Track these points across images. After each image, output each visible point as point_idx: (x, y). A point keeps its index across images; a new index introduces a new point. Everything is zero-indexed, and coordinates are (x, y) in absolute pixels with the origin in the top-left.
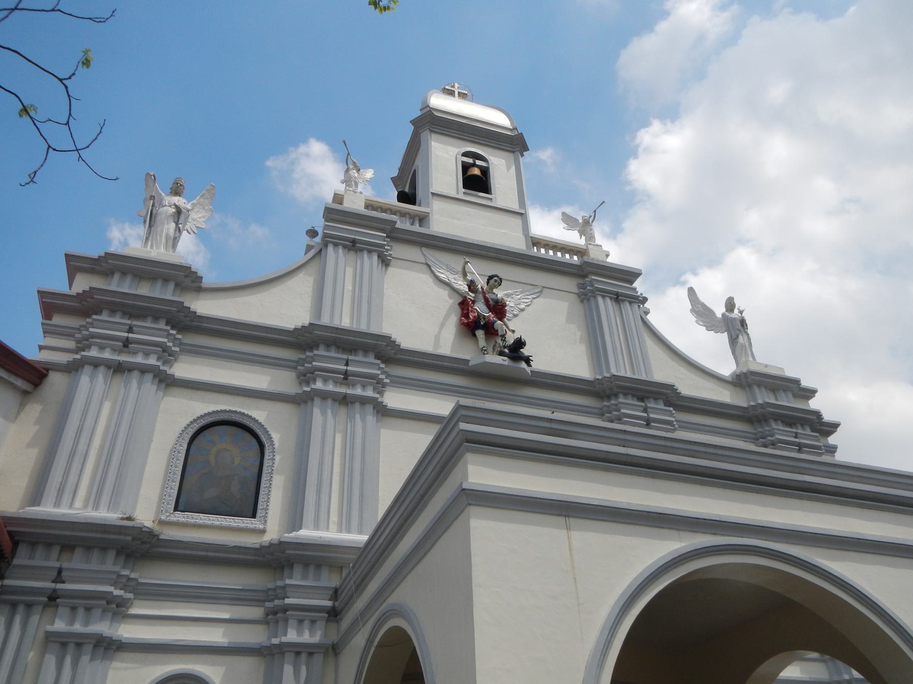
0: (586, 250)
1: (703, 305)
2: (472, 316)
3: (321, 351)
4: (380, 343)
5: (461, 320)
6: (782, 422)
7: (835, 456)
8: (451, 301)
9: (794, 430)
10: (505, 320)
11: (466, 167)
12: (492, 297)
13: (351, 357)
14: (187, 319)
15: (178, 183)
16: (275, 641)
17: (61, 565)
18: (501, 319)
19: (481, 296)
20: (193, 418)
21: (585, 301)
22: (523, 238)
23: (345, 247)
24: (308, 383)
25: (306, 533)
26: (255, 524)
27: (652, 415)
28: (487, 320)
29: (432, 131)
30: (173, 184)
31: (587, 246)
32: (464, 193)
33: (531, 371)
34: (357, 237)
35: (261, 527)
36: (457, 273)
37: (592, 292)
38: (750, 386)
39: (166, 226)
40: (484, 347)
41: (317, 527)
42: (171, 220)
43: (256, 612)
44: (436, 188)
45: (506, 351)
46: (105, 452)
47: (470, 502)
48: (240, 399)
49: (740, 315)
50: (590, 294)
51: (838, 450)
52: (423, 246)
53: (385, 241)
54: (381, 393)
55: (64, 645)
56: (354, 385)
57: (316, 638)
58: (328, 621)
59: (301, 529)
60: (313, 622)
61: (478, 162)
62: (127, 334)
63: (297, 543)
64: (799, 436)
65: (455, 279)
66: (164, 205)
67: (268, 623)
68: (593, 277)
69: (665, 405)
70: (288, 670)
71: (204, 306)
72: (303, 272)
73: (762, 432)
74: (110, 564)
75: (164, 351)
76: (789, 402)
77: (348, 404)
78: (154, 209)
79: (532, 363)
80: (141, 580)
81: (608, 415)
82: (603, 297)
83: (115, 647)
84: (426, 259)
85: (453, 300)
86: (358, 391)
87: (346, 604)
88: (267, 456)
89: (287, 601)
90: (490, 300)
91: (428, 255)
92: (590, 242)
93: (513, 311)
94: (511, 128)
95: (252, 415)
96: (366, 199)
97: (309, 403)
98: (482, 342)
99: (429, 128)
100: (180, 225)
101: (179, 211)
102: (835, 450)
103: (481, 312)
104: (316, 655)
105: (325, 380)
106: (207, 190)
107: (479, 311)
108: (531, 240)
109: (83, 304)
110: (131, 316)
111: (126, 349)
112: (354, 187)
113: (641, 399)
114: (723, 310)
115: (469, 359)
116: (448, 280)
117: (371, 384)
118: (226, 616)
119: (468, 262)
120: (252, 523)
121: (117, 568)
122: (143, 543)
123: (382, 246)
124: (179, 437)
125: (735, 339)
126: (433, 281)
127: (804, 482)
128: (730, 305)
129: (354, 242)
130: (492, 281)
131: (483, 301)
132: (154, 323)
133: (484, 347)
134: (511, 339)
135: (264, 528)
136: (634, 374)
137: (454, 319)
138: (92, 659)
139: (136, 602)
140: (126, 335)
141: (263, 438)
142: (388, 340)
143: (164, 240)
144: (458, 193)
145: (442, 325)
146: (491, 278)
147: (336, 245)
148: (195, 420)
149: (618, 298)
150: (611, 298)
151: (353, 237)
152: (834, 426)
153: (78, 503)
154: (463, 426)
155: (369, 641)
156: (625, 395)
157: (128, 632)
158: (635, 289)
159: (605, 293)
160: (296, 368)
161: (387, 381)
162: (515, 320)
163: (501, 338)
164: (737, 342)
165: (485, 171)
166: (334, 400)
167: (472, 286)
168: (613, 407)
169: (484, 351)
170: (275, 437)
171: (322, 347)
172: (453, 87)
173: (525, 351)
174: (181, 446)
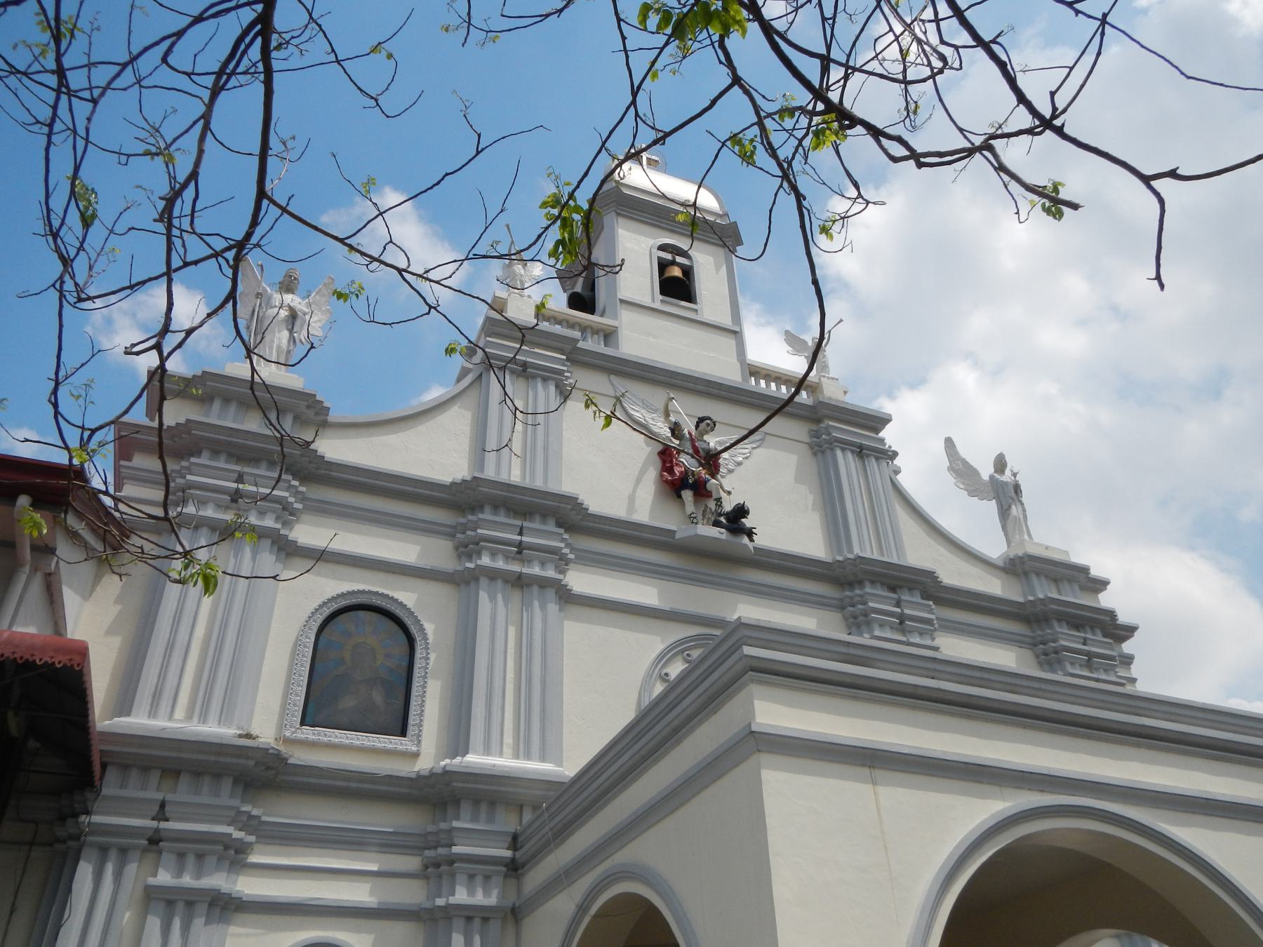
0: (818, 383)
1: (965, 462)
3: (487, 515)
4: (562, 505)
5: (662, 476)
6: (1068, 623)
7: (1130, 668)
8: (649, 449)
9: (1083, 635)
10: (719, 476)
11: (663, 266)
13: (526, 524)
14: (312, 465)
15: (291, 276)
16: (440, 902)
17: (164, 798)
18: (713, 476)
20: (322, 600)
21: (819, 454)
24: (470, 557)
25: (475, 759)
26: (406, 745)
27: (907, 611)
28: (696, 477)
29: (618, 214)
30: (285, 277)
31: (820, 379)
32: (661, 301)
33: (754, 548)
34: (528, 360)
35: (414, 749)
36: (655, 411)
38: (1026, 574)
39: (277, 334)
40: (693, 513)
41: (487, 751)
42: (284, 326)
43: (411, 863)
44: (624, 293)
45: (723, 519)
46: (213, 644)
47: (760, 748)
48: (381, 576)
49: (1013, 478)
50: (826, 445)
51: (1135, 661)
52: (613, 374)
53: (564, 365)
54: (563, 572)
55: (170, 903)
56: (529, 562)
57: (492, 900)
58: (506, 876)
59: (468, 753)
60: (487, 878)
61: (679, 259)
62: (236, 484)
63: (467, 773)
64: (1088, 642)
65: (653, 419)
66: (273, 305)
67: (427, 878)
68: (831, 423)
69: (923, 598)
70: (458, 941)
71: (333, 448)
73: (1042, 636)
74: (226, 797)
75: (284, 509)
76: (1075, 597)
77: (523, 587)
78: (260, 311)
80: (264, 818)
81: (850, 609)
82: (843, 450)
83: (233, 907)
86: (536, 570)
87: (534, 856)
88: (419, 653)
89: (455, 849)
91: (618, 385)
92: (823, 374)
94: (721, 213)
95: (398, 598)
97: (473, 585)
98: (690, 506)
100: (295, 334)
101: (293, 316)
102: (1130, 661)
104: (492, 921)
105: (493, 555)
106: (325, 284)
109: (174, 441)
110: (239, 459)
111: (234, 505)
113: (893, 589)
114: (992, 470)
115: (676, 529)
116: (645, 420)
117: (552, 561)
118: (374, 867)
119: (673, 398)
120: (402, 744)
121: (235, 802)
122: (269, 768)
123: (561, 372)
124: (305, 626)
125: (1007, 510)
127: (1143, 726)
128: (1000, 464)
130: (703, 425)
132: (269, 471)
133: (693, 513)
134: (728, 507)
135: (418, 750)
136: (883, 555)
137: (652, 474)
138: (207, 923)
139: (257, 847)
140: (235, 485)
141: (413, 630)
142: (572, 502)
144: (653, 300)
145: (638, 481)
146: (701, 420)
148: (324, 604)
149: (861, 452)
150: (853, 452)
151: (524, 359)
152: (1130, 631)
153: (180, 713)
154: (748, 650)
155: (582, 909)
156: (873, 582)
157: (249, 886)
158: (882, 441)
159: (845, 445)
160: (453, 536)
161: (572, 556)
162: (729, 476)
163: (716, 502)
164: (1009, 514)
165: (688, 272)
166: (506, 582)
167: (676, 430)
168: (859, 599)
169: (692, 519)
170: (429, 628)
171: (488, 509)
173: (748, 522)
174: (307, 637)
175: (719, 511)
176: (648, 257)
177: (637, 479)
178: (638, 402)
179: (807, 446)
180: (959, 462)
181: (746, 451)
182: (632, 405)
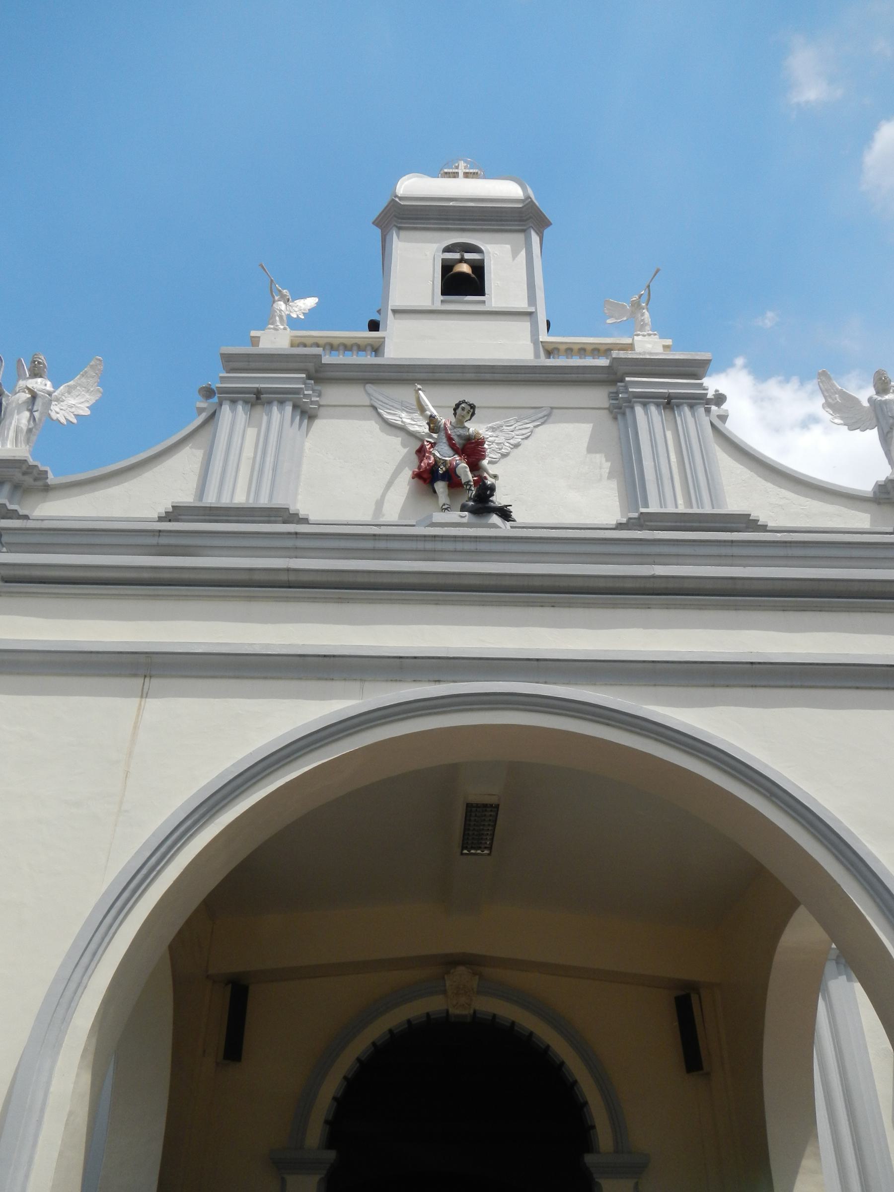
11: (447, 267)
12: (458, 433)
19: (442, 434)
21: (619, 417)
23: (246, 402)
29: (400, 228)
31: (633, 339)
37: (628, 401)
39: (16, 417)
40: (444, 505)
50: (624, 404)
52: (367, 383)
61: (468, 256)
65: (412, 419)
72: (190, 445)
79: (514, 515)
82: (645, 405)
84: (371, 399)
85: (408, 449)
90: (455, 438)
96: (292, 336)
99: (395, 225)
101: (34, 396)
103: (440, 457)
107: (438, 455)
108: (543, 347)
112: (278, 324)
114: (871, 392)
125: (888, 433)
129: (258, 393)
130: (459, 411)
131: (445, 440)
133: (444, 505)
143: (12, 434)
146: (458, 406)
147: (234, 401)
149: (669, 403)
150: (658, 405)
151: (257, 386)
159: (646, 399)
165: (479, 269)
172: (457, 168)
175: (470, 496)
176: (432, 261)
177: (388, 482)
178: (396, 405)
179: (606, 412)
180: (837, 396)
181: (528, 430)
182: (390, 409)
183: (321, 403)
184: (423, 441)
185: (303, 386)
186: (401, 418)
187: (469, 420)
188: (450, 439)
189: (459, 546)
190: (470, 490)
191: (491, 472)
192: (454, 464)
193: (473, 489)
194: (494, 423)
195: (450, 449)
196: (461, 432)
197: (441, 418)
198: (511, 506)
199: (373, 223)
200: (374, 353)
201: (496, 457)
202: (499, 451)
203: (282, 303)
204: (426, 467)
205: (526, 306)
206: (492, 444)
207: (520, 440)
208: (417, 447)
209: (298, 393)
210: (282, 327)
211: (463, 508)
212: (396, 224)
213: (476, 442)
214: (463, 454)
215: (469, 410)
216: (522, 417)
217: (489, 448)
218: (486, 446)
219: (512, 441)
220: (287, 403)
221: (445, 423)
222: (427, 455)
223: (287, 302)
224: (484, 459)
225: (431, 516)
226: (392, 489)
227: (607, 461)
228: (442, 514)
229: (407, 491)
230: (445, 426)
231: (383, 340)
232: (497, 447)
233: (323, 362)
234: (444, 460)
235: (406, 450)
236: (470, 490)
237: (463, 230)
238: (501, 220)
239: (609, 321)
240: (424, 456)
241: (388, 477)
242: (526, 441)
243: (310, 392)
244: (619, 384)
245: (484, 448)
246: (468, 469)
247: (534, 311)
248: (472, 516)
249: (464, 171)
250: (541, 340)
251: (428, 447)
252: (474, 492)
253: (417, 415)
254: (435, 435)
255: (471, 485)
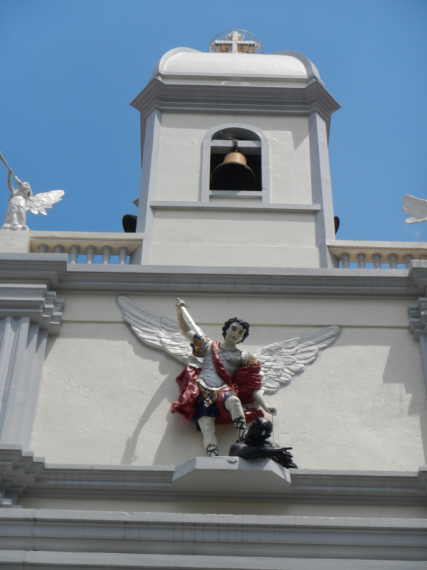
2: (187, 395)
12: (228, 358)
19: (209, 358)
22: (316, 251)
28: (214, 399)
29: (162, 111)
33: (293, 476)
65: (173, 339)
79: (294, 460)
85: (167, 375)
90: (224, 363)
93: (279, 377)
103: (206, 387)
107: (203, 384)
108: (331, 252)
112: (16, 222)
115: (173, 469)
119: (183, 305)
123: (36, 305)
126: (134, 350)
130: (229, 331)
131: (212, 366)
133: (210, 446)
146: (227, 325)
172: (230, 38)
175: (241, 435)
177: (143, 417)
178: (154, 322)
179: (406, 331)
181: (313, 354)
182: (146, 327)
183: (64, 318)
184: (185, 366)
185: (43, 299)
186: (160, 338)
187: (242, 341)
188: (218, 365)
189: (223, 536)
190: (241, 428)
191: (267, 405)
192: (223, 395)
193: (245, 427)
194: (271, 345)
195: (218, 377)
196: (232, 356)
197: (208, 339)
198: (291, 448)
199: (131, 104)
200: (128, 257)
201: (271, 386)
202: (277, 379)
203: (21, 197)
204: (188, 400)
205: (311, 203)
206: (269, 370)
207: (302, 366)
208: (179, 373)
209: (37, 308)
210: (20, 226)
211: (233, 452)
212: (158, 106)
213: (250, 368)
214: (233, 383)
215: (241, 331)
216: (306, 337)
217: (266, 376)
218: (261, 373)
219: (292, 367)
220: (24, 319)
221: (212, 346)
222: (190, 384)
223: (27, 196)
224: (259, 389)
225: (194, 461)
226: (147, 425)
227: (407, 392)
228: (207, 459)
229: (165, 428)
230: (212, 350)
231: (140, 242)
232: (274, 373)
233: (68, 270)
234: (210, 391)
235: (164, 377)
236: (241, 428)
237: (236, 114)
238: (281, 103)
239: (409, 221)
240: (186, 385)
241: (142, 409)
242: (309, 367)
243: (52, 306)
244: (421, 299)
245: (260, 376)
246: (239, 403)
247: (320, 209)
248: (243, 461)
249: (239, 42)
250: (328, 244)
251: (191, 374)
252: (247, 431)
253: (178, 334)
254: (200, 360)
255: (243, 423)
